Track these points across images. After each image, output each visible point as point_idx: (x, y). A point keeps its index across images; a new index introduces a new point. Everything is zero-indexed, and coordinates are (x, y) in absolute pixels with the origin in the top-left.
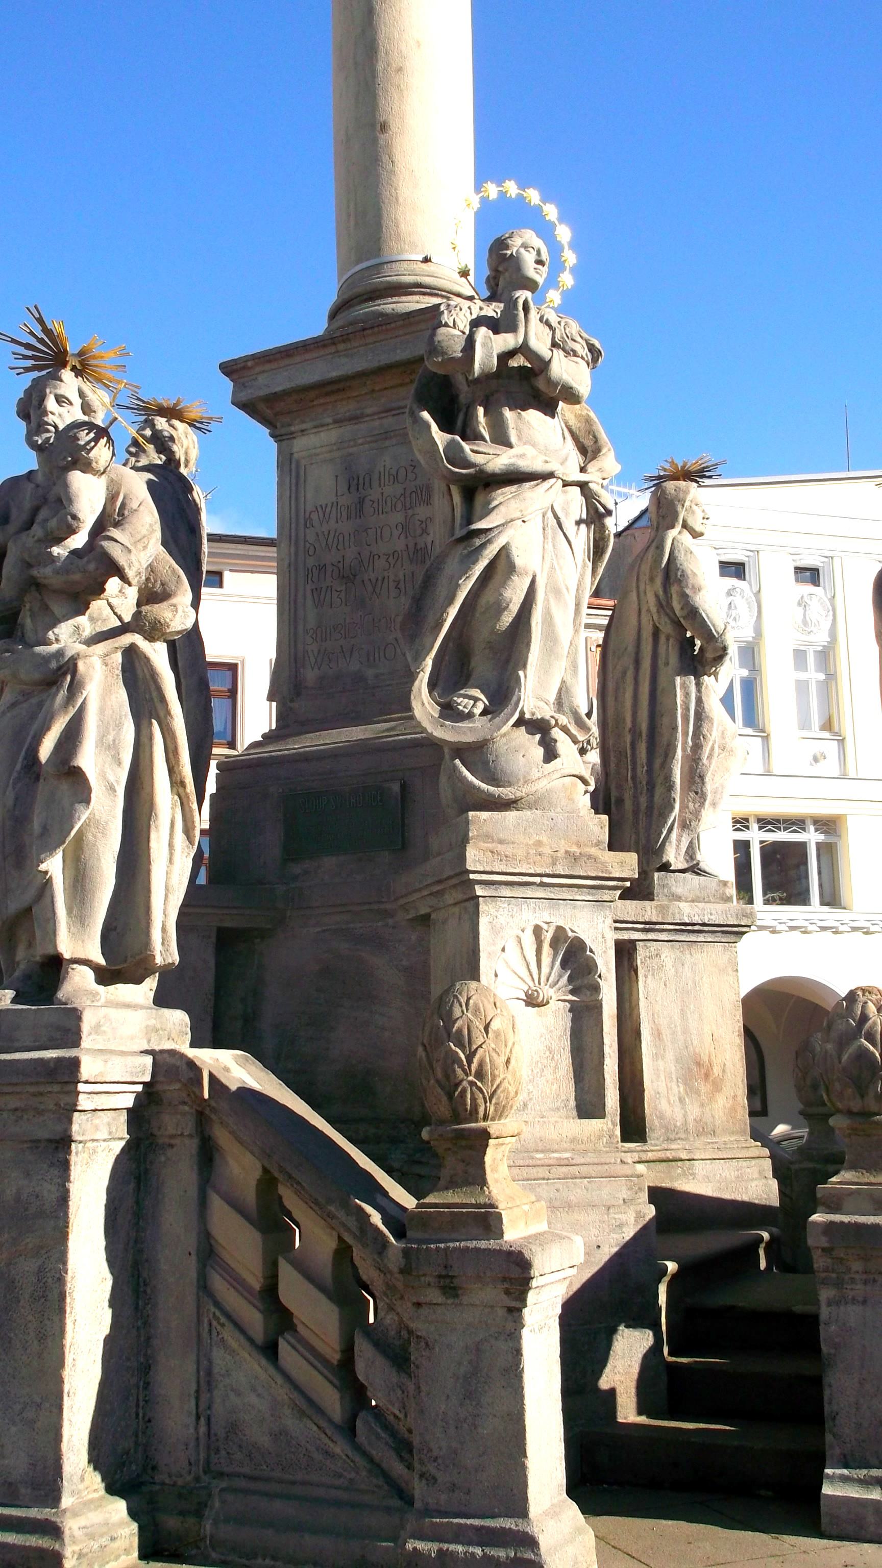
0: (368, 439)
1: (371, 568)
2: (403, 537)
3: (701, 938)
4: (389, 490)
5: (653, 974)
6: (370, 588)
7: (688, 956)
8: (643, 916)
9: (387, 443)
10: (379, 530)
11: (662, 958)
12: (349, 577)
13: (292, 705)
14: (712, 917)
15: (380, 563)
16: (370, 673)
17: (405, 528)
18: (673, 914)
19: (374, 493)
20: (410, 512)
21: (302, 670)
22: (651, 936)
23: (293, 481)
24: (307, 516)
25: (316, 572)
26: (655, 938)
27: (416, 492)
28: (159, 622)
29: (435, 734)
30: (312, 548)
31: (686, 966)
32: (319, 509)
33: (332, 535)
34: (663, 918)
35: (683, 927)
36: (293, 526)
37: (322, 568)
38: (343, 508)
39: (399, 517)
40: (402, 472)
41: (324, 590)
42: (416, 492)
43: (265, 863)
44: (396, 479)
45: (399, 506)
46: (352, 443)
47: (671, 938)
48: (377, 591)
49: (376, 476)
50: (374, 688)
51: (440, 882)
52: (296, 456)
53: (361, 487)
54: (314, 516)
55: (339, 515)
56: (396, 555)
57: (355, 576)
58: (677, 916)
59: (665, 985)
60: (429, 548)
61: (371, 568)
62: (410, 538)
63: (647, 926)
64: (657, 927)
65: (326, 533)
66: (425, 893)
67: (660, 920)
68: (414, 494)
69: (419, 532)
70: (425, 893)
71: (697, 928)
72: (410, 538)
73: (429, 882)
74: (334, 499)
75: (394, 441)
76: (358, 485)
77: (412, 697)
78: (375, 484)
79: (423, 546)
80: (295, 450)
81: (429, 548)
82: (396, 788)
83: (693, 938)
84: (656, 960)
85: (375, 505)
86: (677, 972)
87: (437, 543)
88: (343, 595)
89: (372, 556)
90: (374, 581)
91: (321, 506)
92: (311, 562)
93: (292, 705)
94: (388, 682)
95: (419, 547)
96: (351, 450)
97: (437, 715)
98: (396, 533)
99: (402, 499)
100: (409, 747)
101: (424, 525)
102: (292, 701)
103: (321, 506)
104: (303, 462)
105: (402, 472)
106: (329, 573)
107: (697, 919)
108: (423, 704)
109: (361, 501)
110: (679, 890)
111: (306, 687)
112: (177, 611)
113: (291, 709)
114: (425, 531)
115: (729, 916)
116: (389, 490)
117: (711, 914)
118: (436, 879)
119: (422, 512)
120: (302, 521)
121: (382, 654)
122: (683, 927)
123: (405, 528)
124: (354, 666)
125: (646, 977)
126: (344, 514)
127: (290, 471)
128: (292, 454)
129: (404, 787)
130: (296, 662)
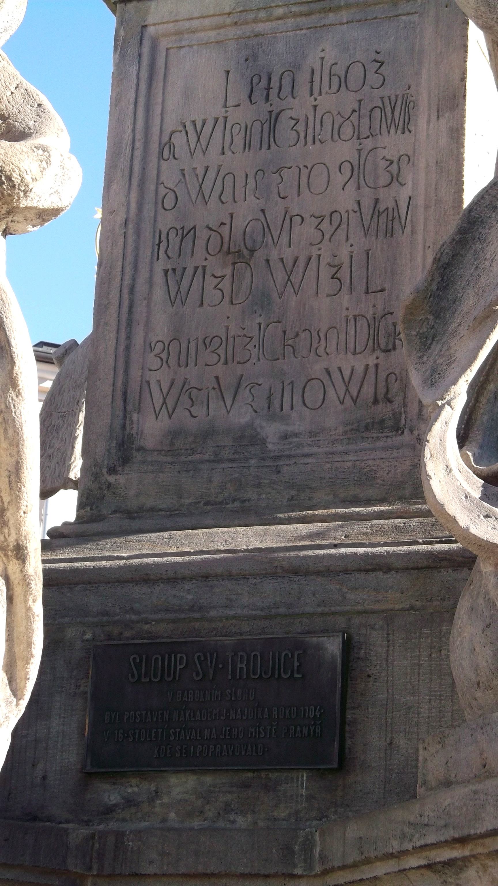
0: (294, 9)
1: (284, 239)
2: (351, 187)
4: (327, 102)
6: (280, 276)
9: (331, 18)
10: (305, 172)
12: (240, 253)
13: (112, 479)
15: (305, 232)
16: (271, 431)
17: (356, 171)
19: (299, 106)
20: (369, 143)
21: (135, 416)
23: (144, 74)
24: (165, 139)
25: (175, 241)
27: (383, 109)
28: (9, 178)
29: (473, 530)
30: (171, 197)
32: (190, 128)
33: (211, 175)
36: (138, 153)
37: (188, 233)
38: (236, 129)
39: (345, 150)
40: (357, 71)
41: (190, 271)
42: (383, 109)
43: (44, 778)
44: (343, 82)
45: (347, 131)
46: (262, 14)
48: (295, 279)
49: (303, 78)
50: (278, 458)
51: (462, 841)
52: (151, 30)
53: (274, 92)
54: (179, 140)
55: (228, 139)
56: (336, 217)
57: (252, 251)
60: (403, 211)
61: (284, 239)
62: (365, 190)
65: (200, 171)
66: (413, 862)
68: (377, 111)
69: (384, 178)
70: (413, 862)
72: (365, 190)
73: (431, 839)
74: (220, 112)
75: (344, 15)
76: (268, 88)
77: (427, 454)
78: (303, 89)
79: (391, 204)
80: (150, 20)
81: (403, 211)
82: (333, 647)
85: (301, 127)
87: (421, 201)
88: (226, 285)
89: (288, 217)
90: (289, 263)
91: (194, 122)
92: (167, 221)
93: (112, 479)
94: (307, 450)
95: (382, 207)
96: (260, 27)
97: (477, 494)
98: (339, 179)
99: (354, 118)
100: (359, 571)
101: (395, 166)
102: (112, 471)
103: (194, 122)
104: (164, 44)
105: (357, 71)
106: (200, 244)
108: (449, 470)
109: (274, 119)
111: (141, 449)
112: (48, 163)
113: (109, 485)
114: (395, 179)
116: (327, 102)
118: (452, 833)
119: (392, 144)
120: (154, 147)
121: (297, 398)
123: (356, 171)
124: (241, 415)
126: (239, 140)
127: (140, 55)
128: (145, 27)
129: (348, 646)
130: (125, 401)
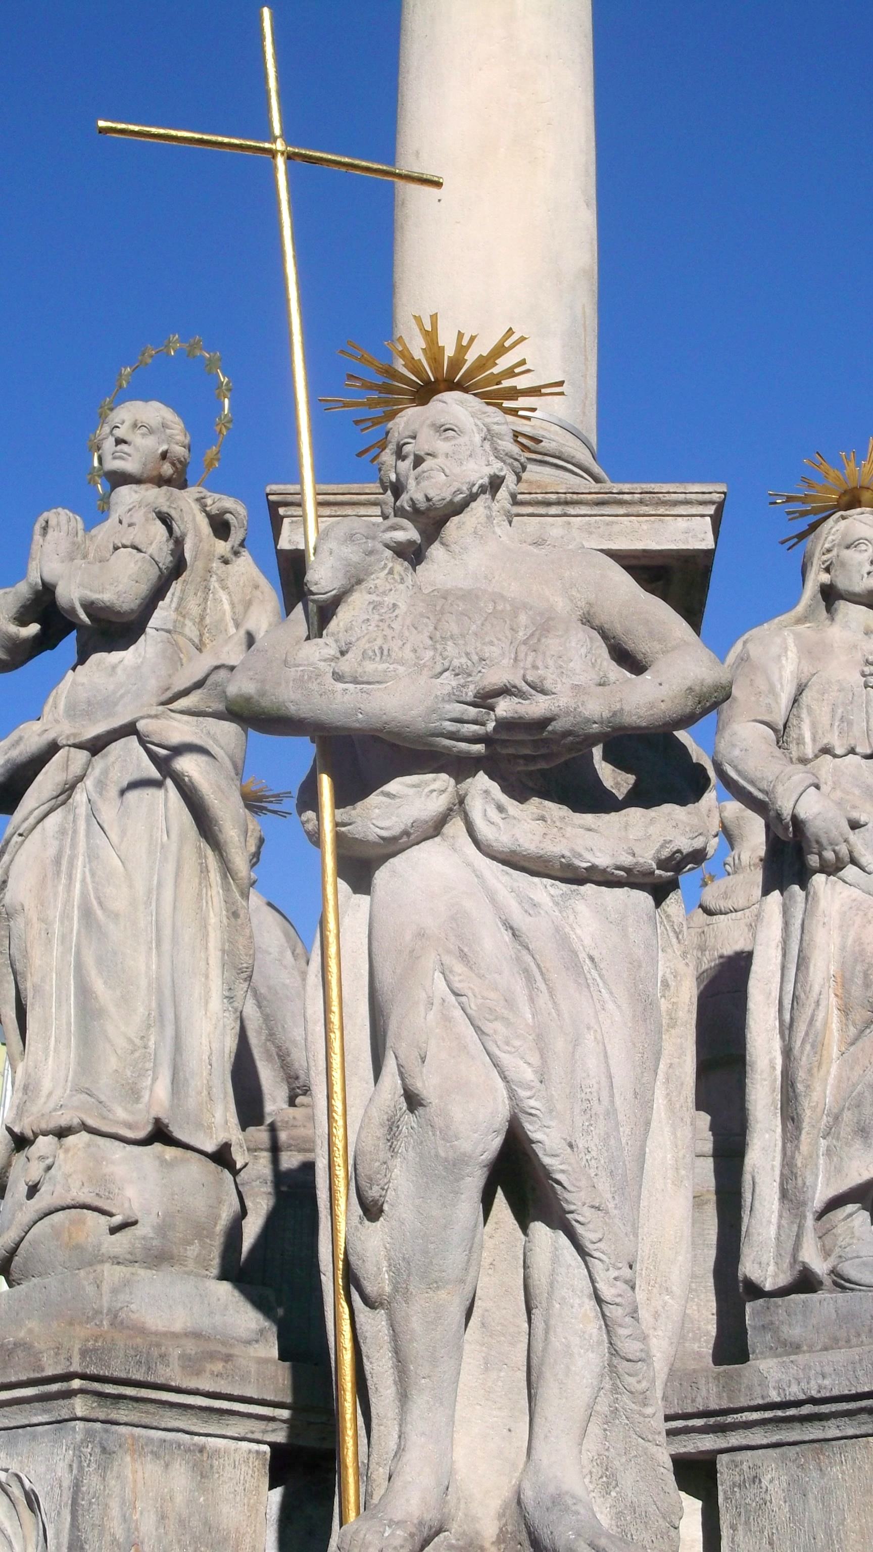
3: (831, 1430)
5: (747, 1523)
7: (815, 1474)
8: (693, 1401)
11: (765, 1482)
14: (827, 1382)
18: (750, 1388)
22: (735, 1439)
26: (744, 1442)
31: (810, 1496)
34: (730, 1399)
35: (779, 1413)
47: (775, 1439)
58: (758, 1390)
59: (771, 1543)
63: (712, 1421)
64: (730, 1419)
67: (725, 1404)
71: (807, 1409)
83: (814, 1432)
84: (754, 1490)
86: (792, 1510)
107: (795, 1392)
110: (793, 1332)
115: (860, 1373)
117: (824, 1377)
122: (779, 1413)
125: (734, 1527)
